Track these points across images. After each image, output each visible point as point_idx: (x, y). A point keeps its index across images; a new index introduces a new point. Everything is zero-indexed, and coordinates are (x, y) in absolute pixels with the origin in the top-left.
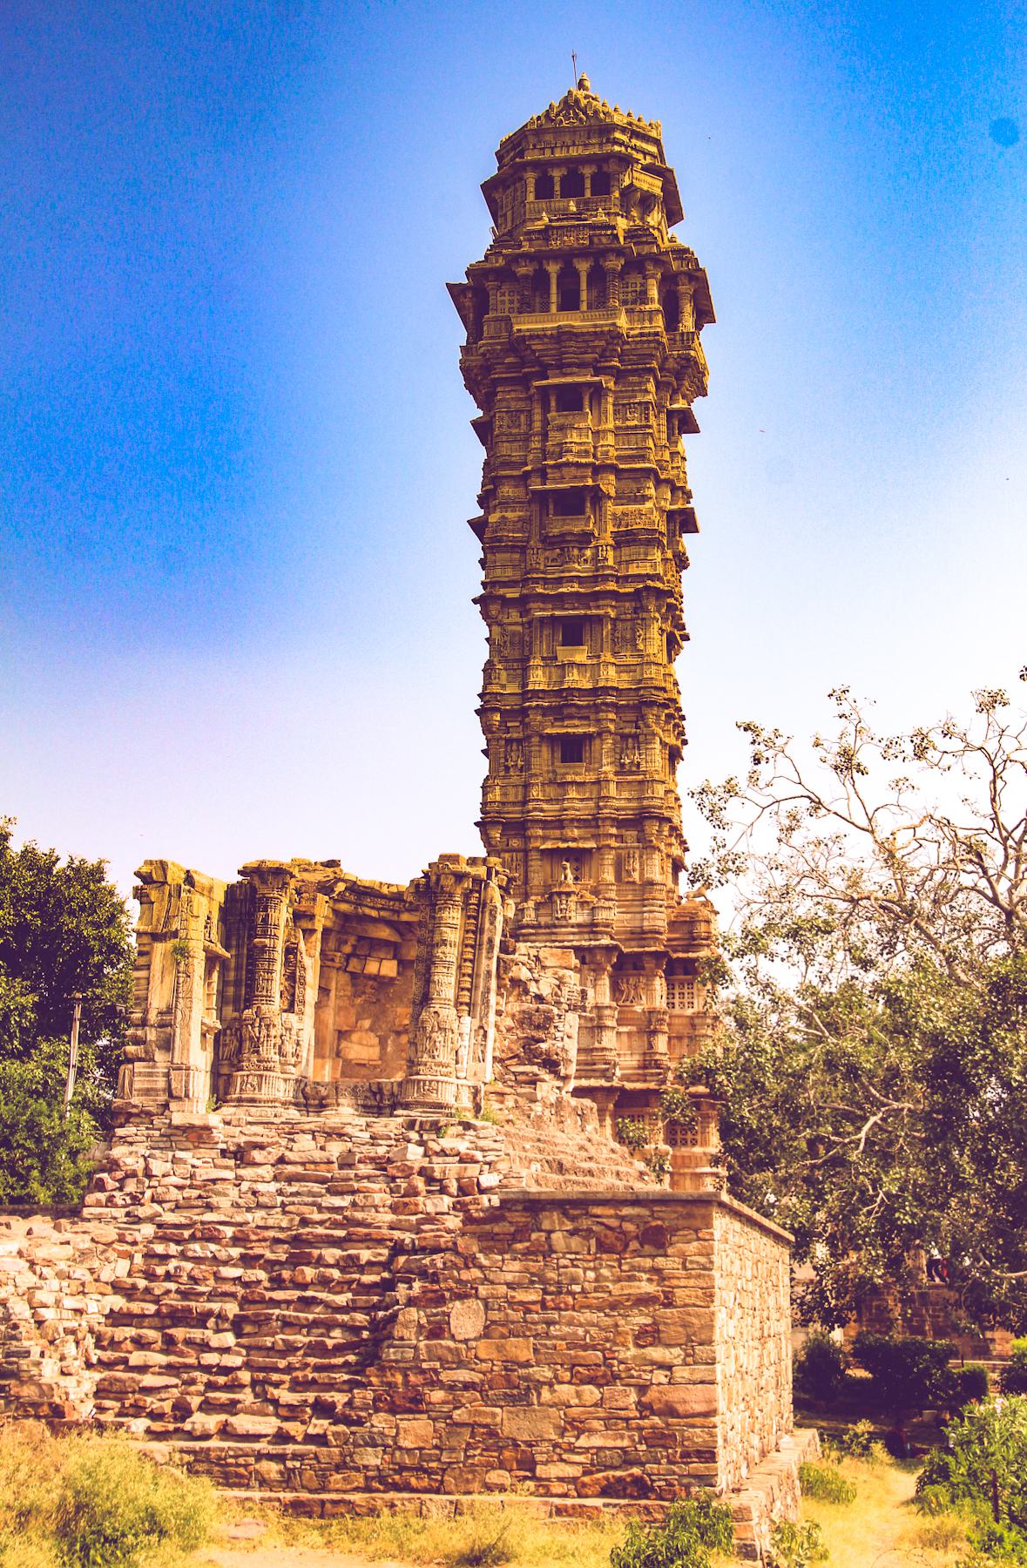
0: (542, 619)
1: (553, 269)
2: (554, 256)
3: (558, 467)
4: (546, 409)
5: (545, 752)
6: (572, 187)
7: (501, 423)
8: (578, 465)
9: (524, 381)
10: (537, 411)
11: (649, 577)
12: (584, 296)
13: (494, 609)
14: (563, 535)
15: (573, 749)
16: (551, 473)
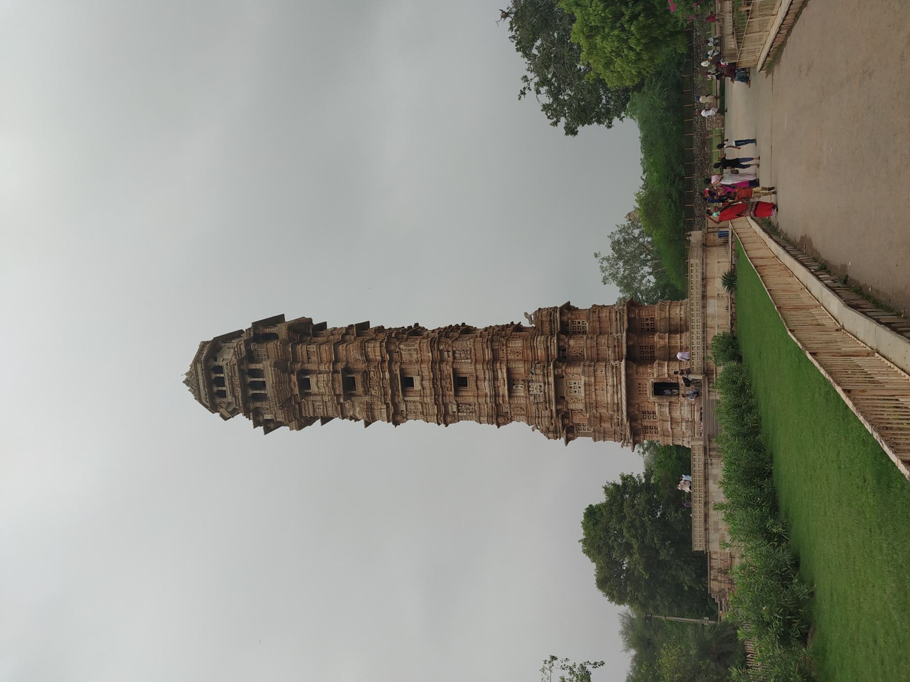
0: (404, 395)
1: (251, 392)
2: (244, 392)
3: (334, 389)
4: (309, 394)
5: (464, 394)
6: (220, 382)
7: (320, 412)
8: (333, 380)
9: (299, 404)
10: (312, 398)
11: (381, 347)
12: (261, 380)
13: (399, 418)
14: (363, 386)
15: (460, 382)
16: (338, 392)
